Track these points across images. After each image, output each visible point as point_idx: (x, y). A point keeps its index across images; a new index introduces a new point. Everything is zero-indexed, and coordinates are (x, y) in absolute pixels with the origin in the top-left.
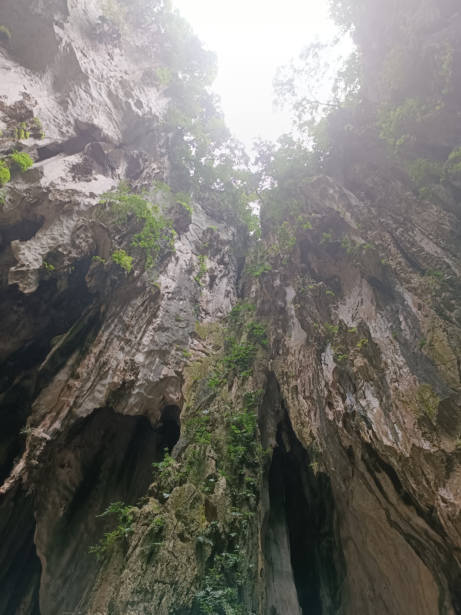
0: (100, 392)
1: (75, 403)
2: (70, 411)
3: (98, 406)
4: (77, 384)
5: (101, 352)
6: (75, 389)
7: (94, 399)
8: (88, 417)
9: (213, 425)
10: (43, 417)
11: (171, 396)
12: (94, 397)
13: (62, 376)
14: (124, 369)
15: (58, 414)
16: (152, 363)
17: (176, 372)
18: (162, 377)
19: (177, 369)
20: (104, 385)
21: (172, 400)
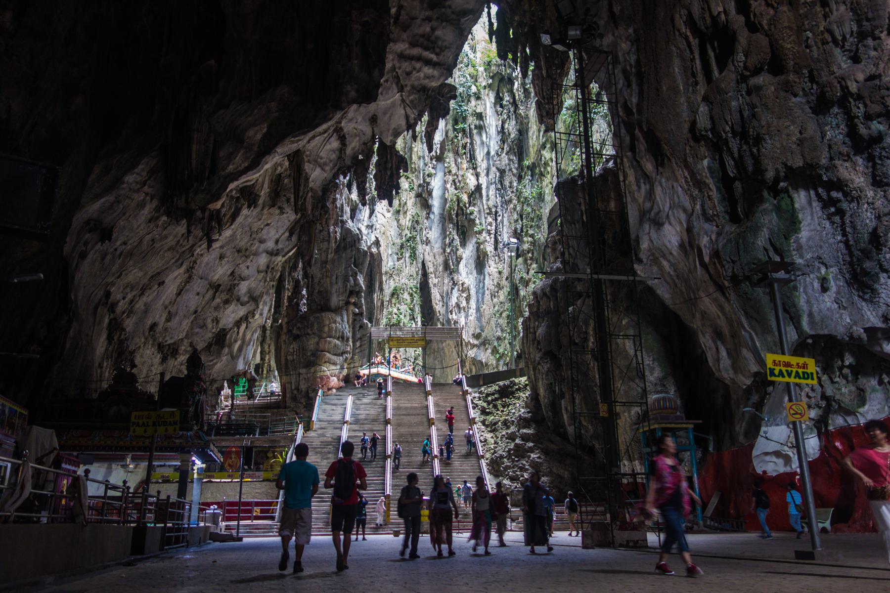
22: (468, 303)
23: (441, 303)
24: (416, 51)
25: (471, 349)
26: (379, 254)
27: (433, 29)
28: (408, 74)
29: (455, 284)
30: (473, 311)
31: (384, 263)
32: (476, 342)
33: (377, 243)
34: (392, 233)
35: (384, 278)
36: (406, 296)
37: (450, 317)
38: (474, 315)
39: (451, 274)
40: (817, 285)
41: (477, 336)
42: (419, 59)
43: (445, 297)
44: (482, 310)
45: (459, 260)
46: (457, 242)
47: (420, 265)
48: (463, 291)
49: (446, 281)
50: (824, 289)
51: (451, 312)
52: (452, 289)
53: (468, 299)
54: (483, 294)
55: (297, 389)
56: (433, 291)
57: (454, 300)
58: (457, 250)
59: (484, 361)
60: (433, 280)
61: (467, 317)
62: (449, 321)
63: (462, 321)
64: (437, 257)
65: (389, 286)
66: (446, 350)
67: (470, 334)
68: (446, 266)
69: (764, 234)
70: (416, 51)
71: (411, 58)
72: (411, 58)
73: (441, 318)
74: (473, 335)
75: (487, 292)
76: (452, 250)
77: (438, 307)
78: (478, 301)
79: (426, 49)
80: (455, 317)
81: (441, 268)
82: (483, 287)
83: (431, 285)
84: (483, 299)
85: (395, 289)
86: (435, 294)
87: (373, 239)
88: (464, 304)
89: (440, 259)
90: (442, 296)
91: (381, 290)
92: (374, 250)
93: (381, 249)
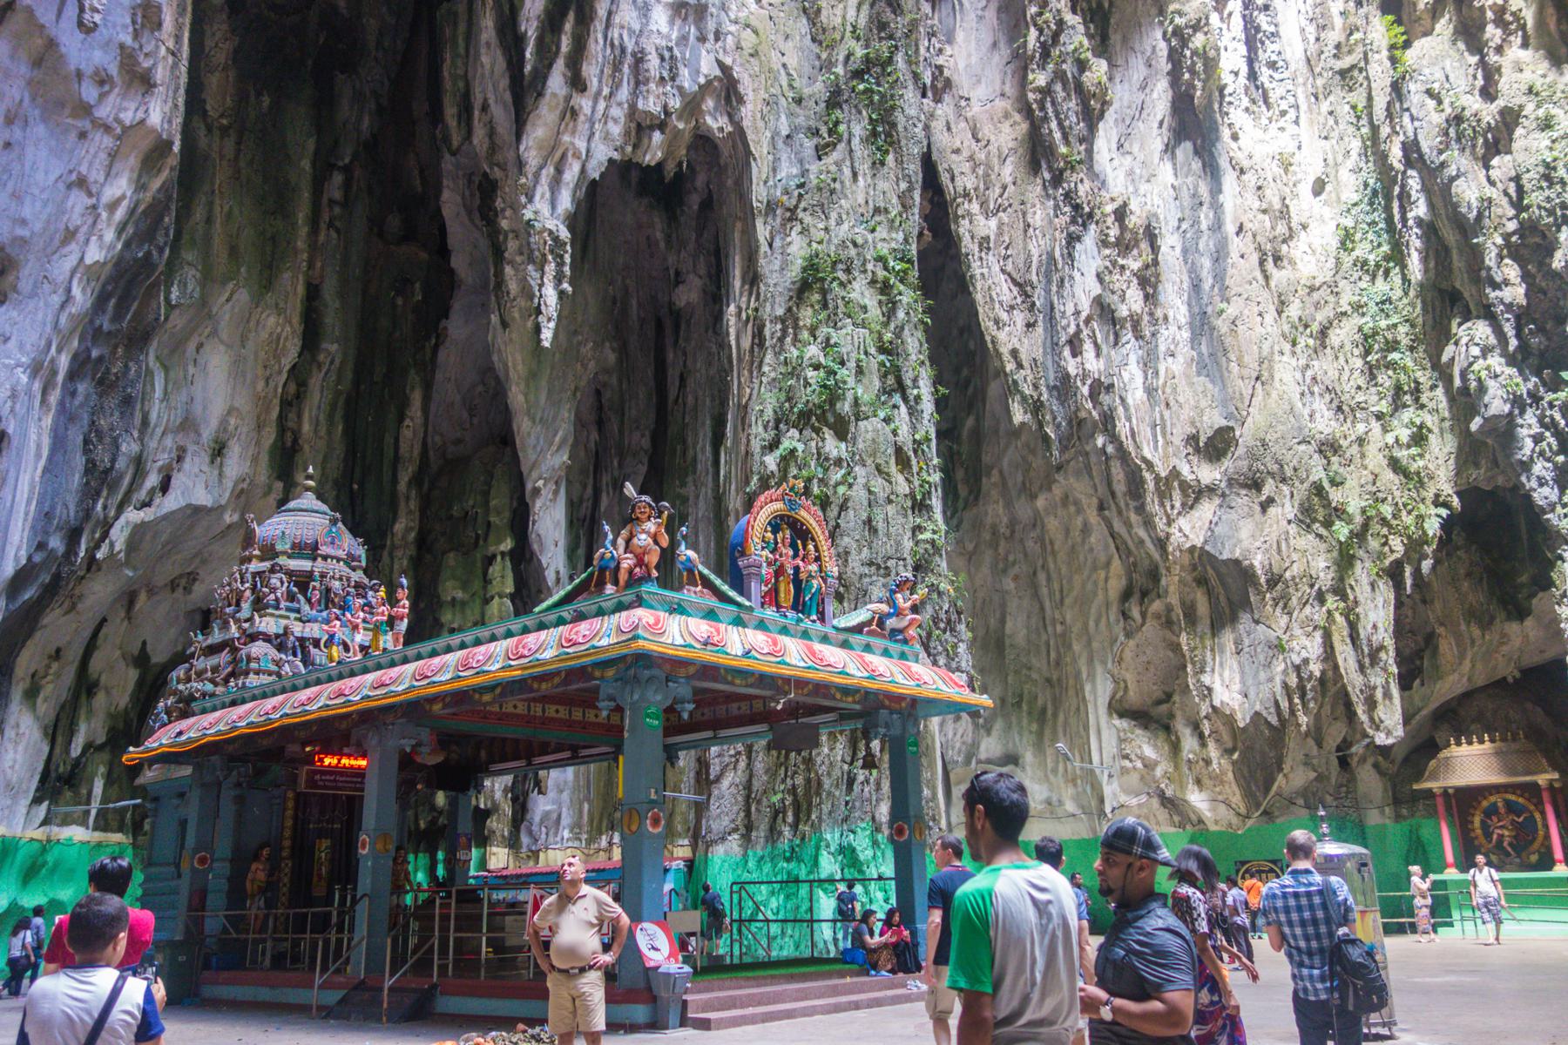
0: (615, 121)
1: (588, 151)
2: (583, 170)
3: (616, 156)
4: (584, 103)
5: (610, 13)
6: (582, 118)
7: (607, 137)
8: (602, 175)
9: (848, 271)
10: (537, 175)
11: (709, 120)
12: (607, 133)
13: (556, 82)
14: (662, 78)
15: (559, 171)
16: (683, 39)
17: (720, 64)
18: (702, 80)
19: (721, 57)
20: (620, 104)
21: (709, 129)
22: (1150, 298)
23: (1020, 318)
25: (1188, 507)
26: (740, 133)
29: (1082, 216)
30: (1175, 333)
31: (759, 170)
32: (1208, 474)
33: (728, 90)
34: (792, 61)
35: (762, 231)
36: (861, 292)
37: (1072, 367)
38: (1185, 351)
39: (1057, 180)
41: (1216, 446)
43: (1037, 290)
44: (1222, 325)
45: (1092, 111)
46: (1077, 37)
47: (914, 168)
48: (1124, 246)
49: (1038, 217)
51: (1075, 344)
52: (1073, 239)
53: (1148, 282)
54: (1220, 256)
56: (976, 269)
57: (1083, 289)
58: (1082, 66)
59: (1258, 561)
61: (1149, 363)
62: (1064, 387)
64: (986, 131)
65: (783, 257)
66: (1052, 524)
68: (1037, 152)
73: (1025, 380)
74: (1192, 439)
75: (1236, 245)
76: (1059, 75)
77: (1011, 335)
78: (1196, 286)
80: (1093, 364)
82: (1217, 226)
83: (968, 245)
84: (1219, 277)
85: (811, 266)
86: (991, 283)
87: (708, 67)
88: (1133, 302)
89: (1007, 135)
90: (1023, 287)
91: (753, 279)
92: (716, 123)
93: (749, 112)
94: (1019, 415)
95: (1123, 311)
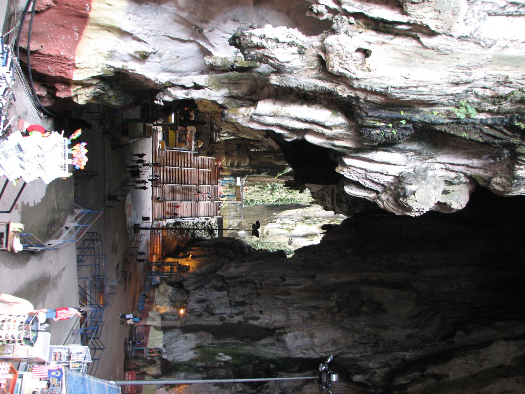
23: (287, 215)
24: (335, 196)
27: (345, 203)
28: (327, 193)
40: (201, 294)
41: (267, 234)
42: (333, 197)
43: (289, 217)
48: (292, 227)
50: (200, 295)
55: (217, 149)
57: (286, 221)
60: (300, 211)
62: (276, 218)
63: (275, 225)
67: (269, 230)
69: (216, 283)
70: (335, 196)
71: (332, 194)
72: (332, 194)
77: (285, 213)
79: (337, 200)
81: (306, 215)
89: (311, 215)
94: (274, 214)
95: (284, 225)
